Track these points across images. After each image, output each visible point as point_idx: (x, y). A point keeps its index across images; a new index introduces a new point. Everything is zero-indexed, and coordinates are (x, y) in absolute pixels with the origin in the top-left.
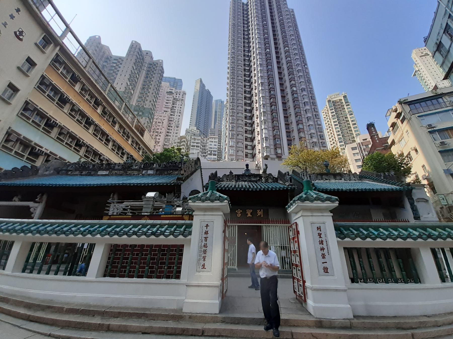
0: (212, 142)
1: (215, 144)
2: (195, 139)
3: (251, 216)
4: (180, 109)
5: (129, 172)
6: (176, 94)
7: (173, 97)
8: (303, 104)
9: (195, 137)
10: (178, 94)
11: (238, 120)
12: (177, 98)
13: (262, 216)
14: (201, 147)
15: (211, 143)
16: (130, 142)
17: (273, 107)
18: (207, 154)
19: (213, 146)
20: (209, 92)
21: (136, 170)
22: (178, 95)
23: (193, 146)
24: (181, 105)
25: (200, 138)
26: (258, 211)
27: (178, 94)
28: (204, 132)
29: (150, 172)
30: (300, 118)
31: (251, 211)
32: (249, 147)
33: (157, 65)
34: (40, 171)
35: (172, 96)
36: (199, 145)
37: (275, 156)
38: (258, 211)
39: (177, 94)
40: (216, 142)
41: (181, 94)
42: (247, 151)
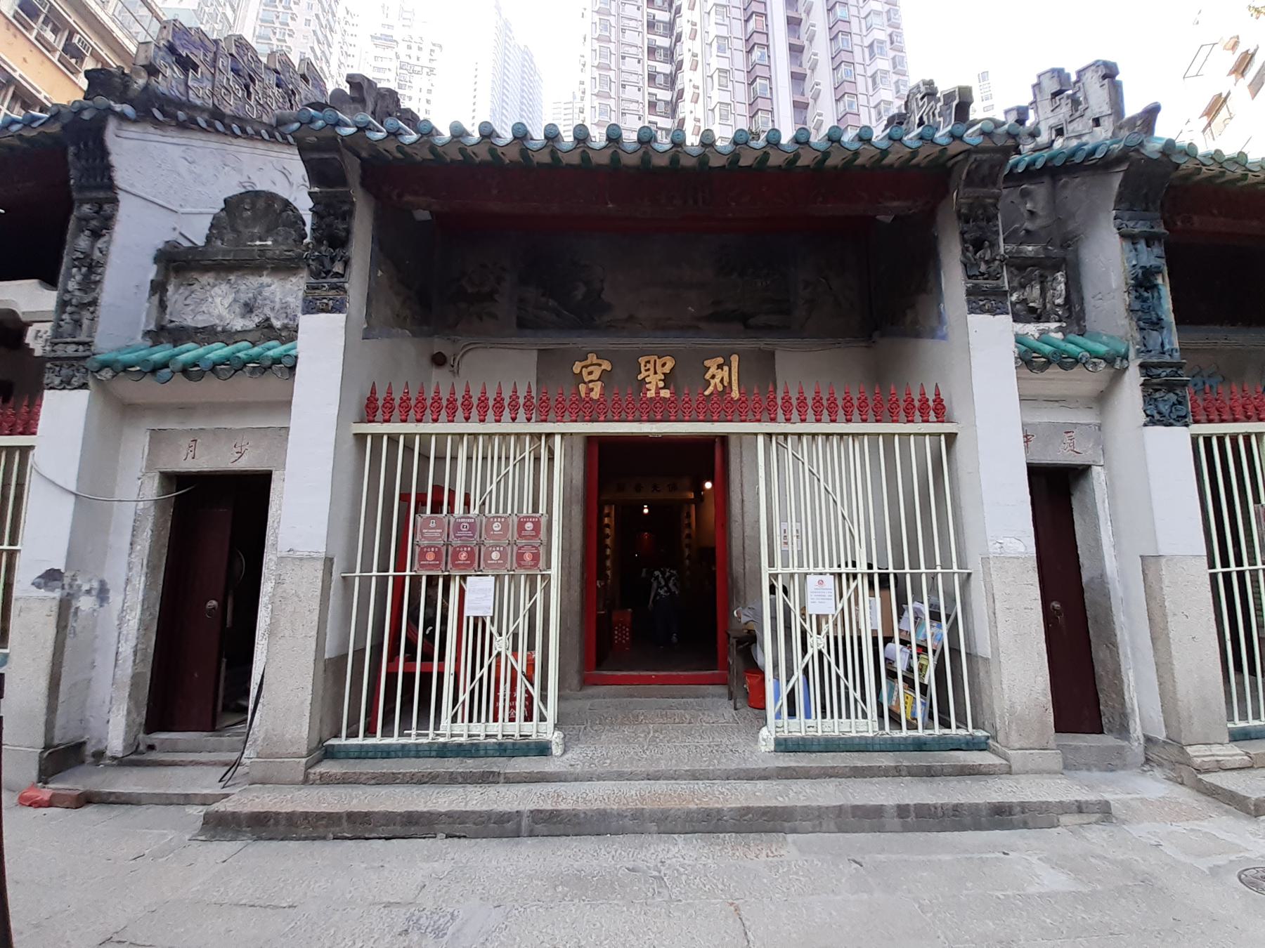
3: (665, 394)
4: (428, 107)
7: (398, 57)
8: (866, 51)
10: (415, 46)
12: (413, 61)
13: (735, 394)
17: (757, 53)
20: (527, 56)
24: (429, 91)
26: (712, 364)
27: (415, 46)
30: (851, 105)
31: (670, 365)
35: (390, 53)
38: (712, 364)
39: (409, 47)
41: (427, 47)
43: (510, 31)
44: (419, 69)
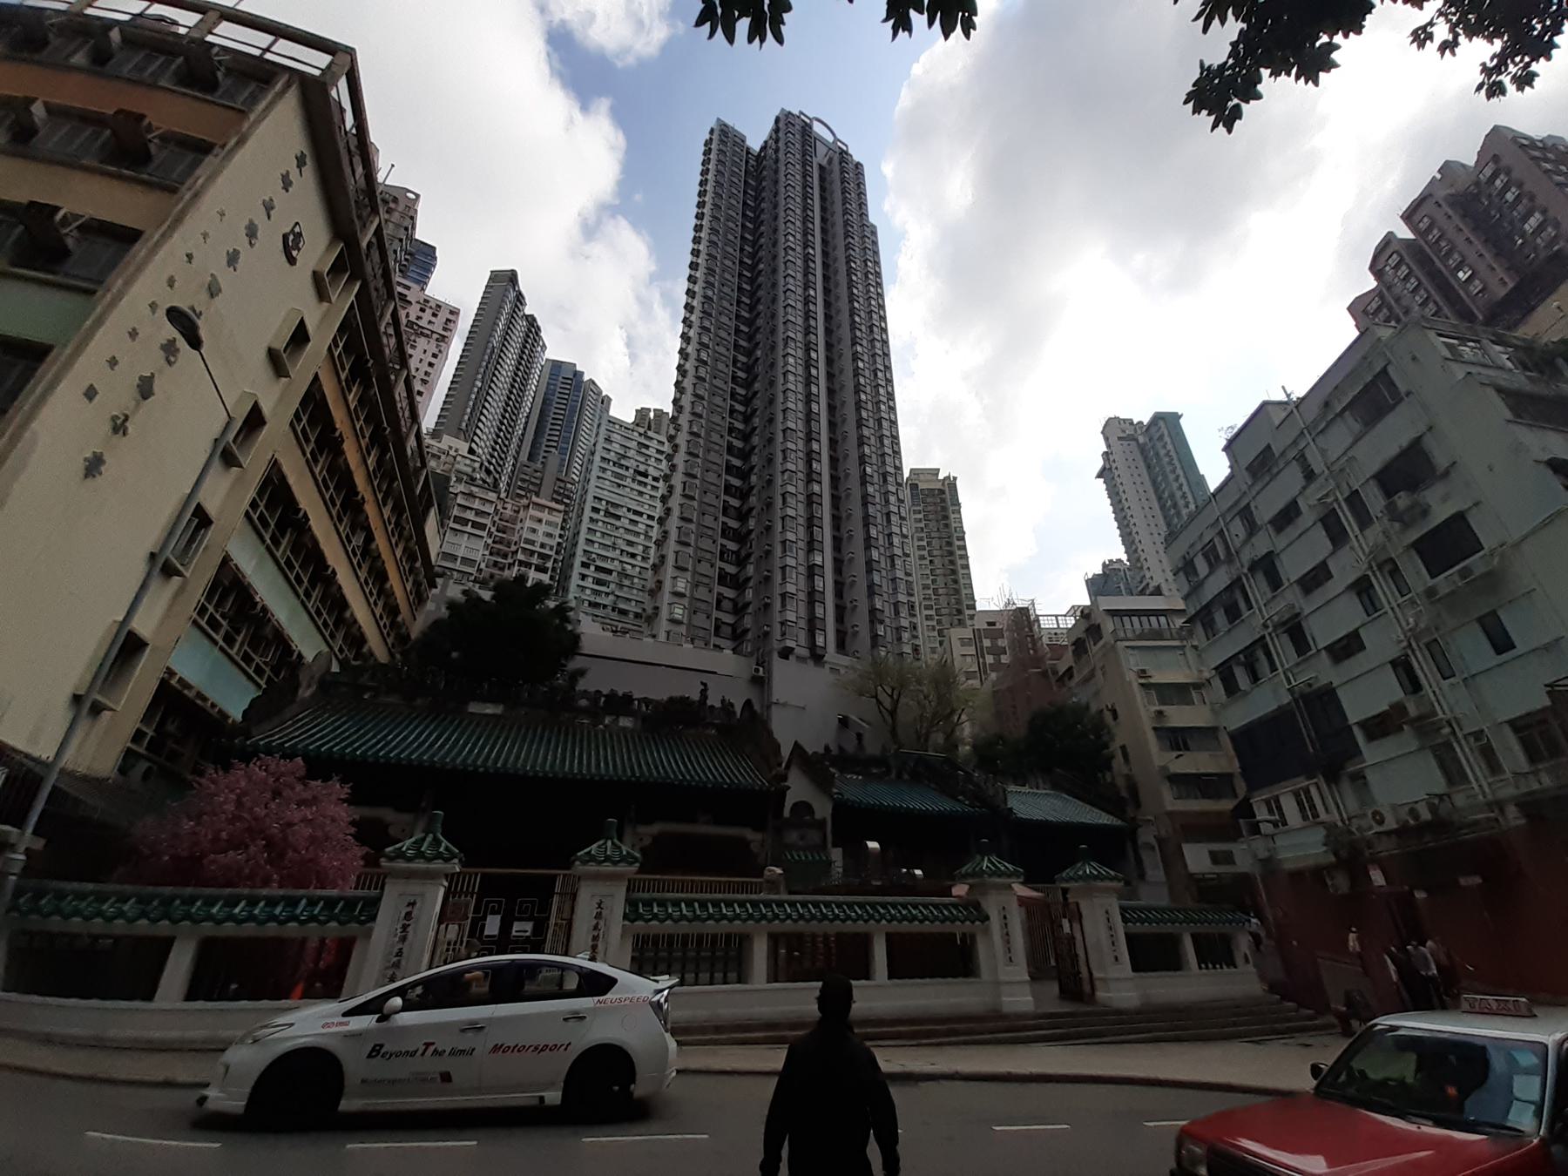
0: (540, 521)
1: (550, 530)
2: (471, 495)
4: (429, 370)
5: (566, 715)
6: (419, 306)
9: (475, 489)
10: (428, 311)
11: (704, 514)
12: (423, 323)
14: (493, 529)
15: (536, 526)
16: (399, 553)
18: (510, 561)
19: (540, 538)
21: (584, 711)
22: (427, 316)
23: (458, 520)
25: (492, 496)
28: (490, 463)
29: (625, 722)
32: (727, 605)
33: (392, 205)
34: (300, 691)
36: (487, 521)
37: (805, 652)
39: (422, 310)
40: (555, 525)
42: (721, 615)
43: (521, 304)
44: (429, 333)
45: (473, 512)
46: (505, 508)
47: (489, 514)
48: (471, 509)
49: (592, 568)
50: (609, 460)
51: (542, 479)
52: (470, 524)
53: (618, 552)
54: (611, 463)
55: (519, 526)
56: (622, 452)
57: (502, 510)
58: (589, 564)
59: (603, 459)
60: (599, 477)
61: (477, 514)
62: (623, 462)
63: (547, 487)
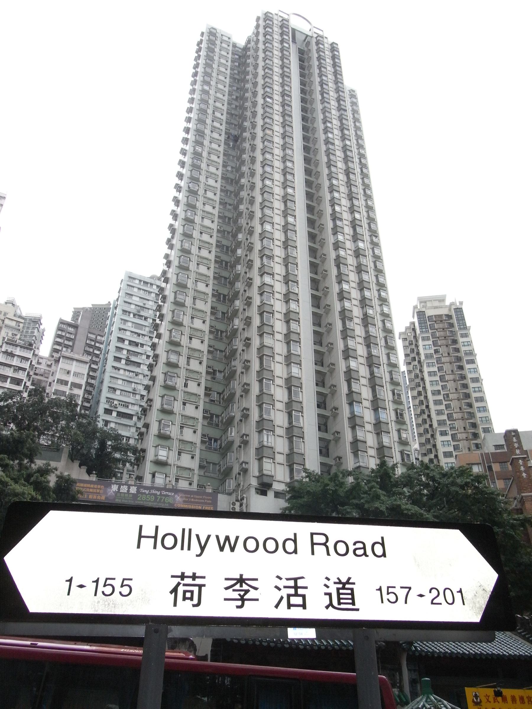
14: (29, 384)
45: (12, 369)
46: (39, 363)
47: (24, 369)
48: (10, 366)
49: (114, 414)
50: (130, 313)
51: (76, 335)
52: (9, 380)
53: (138, 397)
54: (132, 315)
55: (50, 380)
56: (142, 305)
57: (36, 366)
58: (112, 411)
59: (124, 311)
60: (120, 329)
61: (15, 370)
62: (142, 313)
63: (80, 344)
